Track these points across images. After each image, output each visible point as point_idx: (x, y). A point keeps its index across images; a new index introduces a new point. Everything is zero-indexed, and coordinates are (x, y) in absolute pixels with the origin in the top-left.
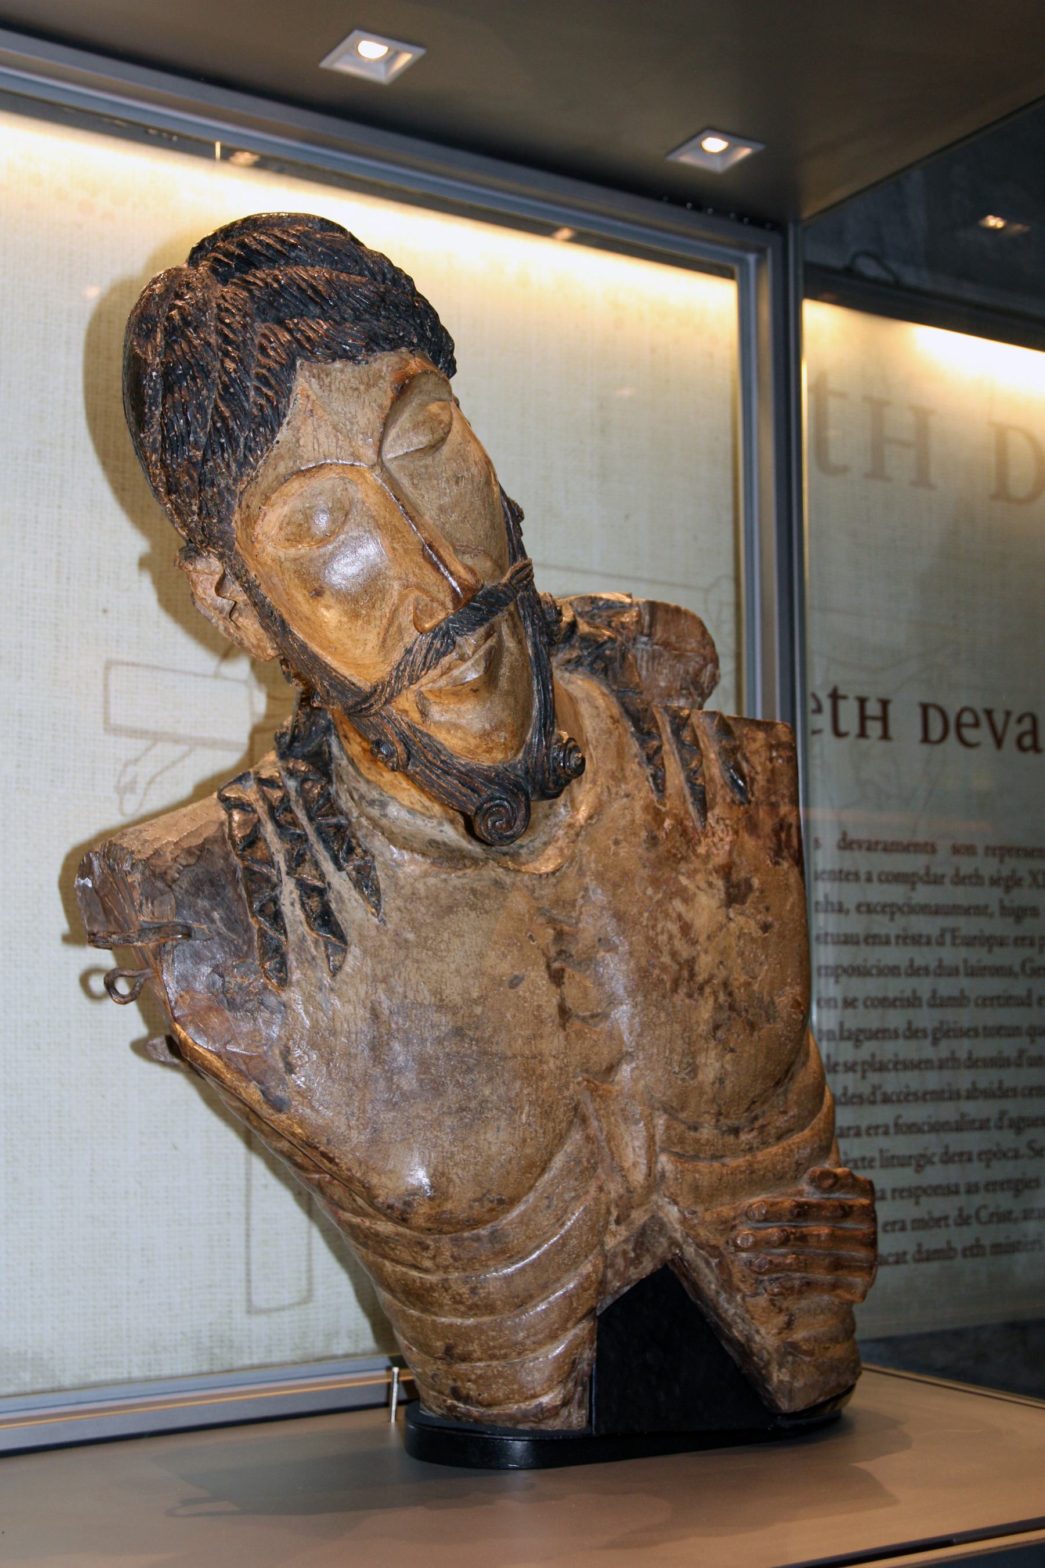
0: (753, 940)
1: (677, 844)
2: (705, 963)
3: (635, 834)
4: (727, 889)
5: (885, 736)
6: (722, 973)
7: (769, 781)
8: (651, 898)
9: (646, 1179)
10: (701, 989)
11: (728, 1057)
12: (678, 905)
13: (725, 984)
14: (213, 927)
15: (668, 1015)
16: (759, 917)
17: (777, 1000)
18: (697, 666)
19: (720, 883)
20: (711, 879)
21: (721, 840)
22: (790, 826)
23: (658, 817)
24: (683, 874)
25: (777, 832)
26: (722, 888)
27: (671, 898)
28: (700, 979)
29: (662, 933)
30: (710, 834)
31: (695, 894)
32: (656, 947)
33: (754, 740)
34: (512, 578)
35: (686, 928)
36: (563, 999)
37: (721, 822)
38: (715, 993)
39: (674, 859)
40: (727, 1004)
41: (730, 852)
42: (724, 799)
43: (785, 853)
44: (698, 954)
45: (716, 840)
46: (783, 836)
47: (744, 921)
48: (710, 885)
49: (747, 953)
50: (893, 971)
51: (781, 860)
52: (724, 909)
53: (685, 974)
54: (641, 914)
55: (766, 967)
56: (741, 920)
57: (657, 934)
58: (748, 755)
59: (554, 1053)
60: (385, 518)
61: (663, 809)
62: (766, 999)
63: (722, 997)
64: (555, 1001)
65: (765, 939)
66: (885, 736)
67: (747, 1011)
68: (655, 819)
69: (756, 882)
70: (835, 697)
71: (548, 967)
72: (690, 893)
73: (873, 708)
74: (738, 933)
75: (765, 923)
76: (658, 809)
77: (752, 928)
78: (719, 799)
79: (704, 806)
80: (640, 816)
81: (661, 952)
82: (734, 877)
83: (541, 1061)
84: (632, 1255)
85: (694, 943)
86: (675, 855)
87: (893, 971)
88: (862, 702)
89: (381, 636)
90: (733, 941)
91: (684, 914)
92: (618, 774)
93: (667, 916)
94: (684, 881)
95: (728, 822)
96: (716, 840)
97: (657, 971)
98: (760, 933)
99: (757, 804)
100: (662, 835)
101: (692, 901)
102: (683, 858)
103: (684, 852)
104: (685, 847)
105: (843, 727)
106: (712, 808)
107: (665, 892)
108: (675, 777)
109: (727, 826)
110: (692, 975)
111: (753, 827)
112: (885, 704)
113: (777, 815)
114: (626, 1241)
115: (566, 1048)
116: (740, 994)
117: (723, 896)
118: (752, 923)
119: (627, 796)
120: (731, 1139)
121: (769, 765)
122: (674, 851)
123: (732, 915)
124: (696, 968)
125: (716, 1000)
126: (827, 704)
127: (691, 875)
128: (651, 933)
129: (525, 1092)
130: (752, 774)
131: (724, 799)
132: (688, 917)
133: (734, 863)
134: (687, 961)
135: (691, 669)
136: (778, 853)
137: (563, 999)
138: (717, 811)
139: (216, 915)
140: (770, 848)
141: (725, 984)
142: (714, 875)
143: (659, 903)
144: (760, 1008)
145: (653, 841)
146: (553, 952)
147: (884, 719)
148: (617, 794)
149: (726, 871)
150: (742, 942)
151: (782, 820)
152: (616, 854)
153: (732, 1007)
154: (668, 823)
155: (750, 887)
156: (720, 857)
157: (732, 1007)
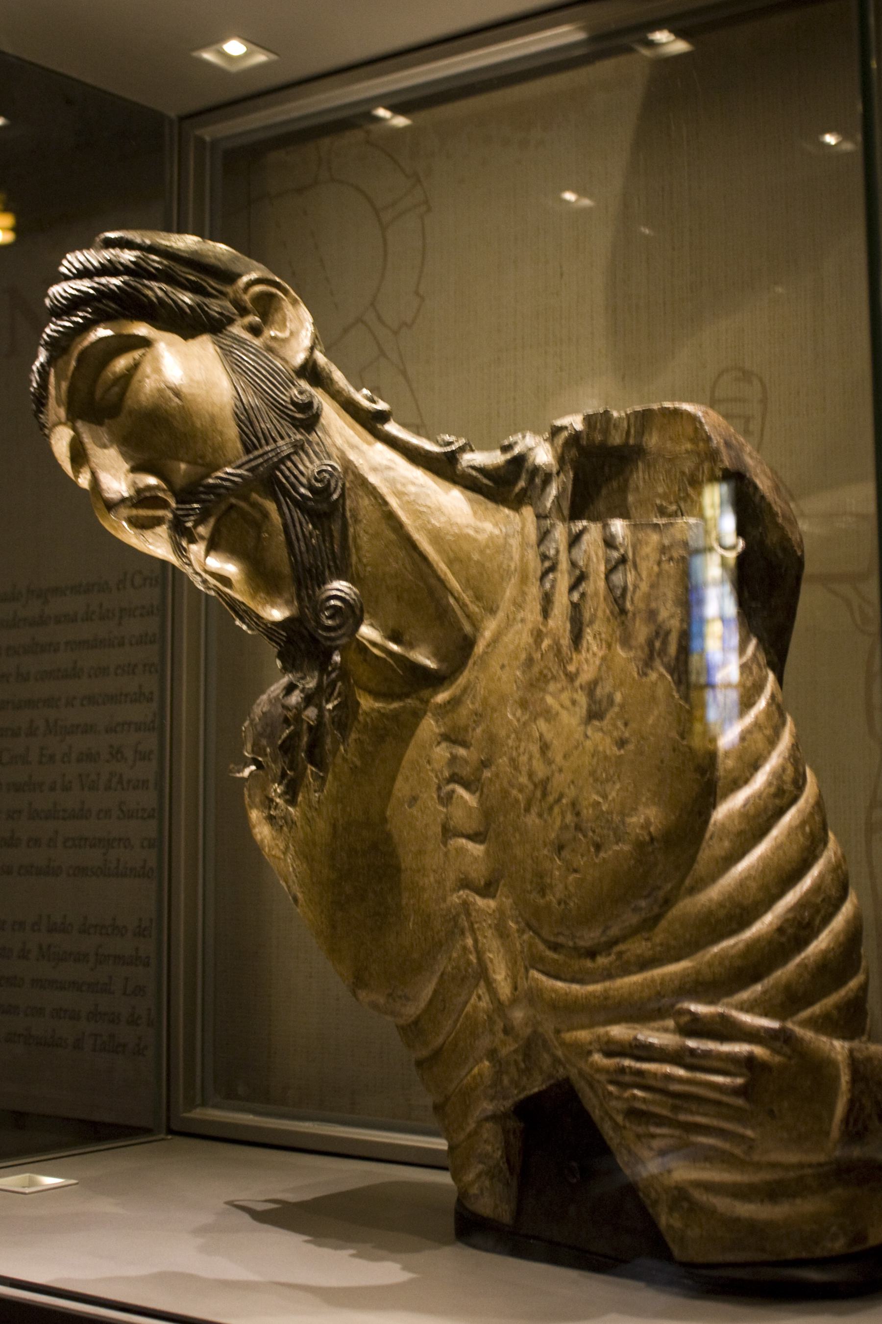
0: (606, 758)
2: (559, 781)
4: (589, 705)
6: (571, 792)
7: (652, 586)
9: (512, 993)
10: (551, 809)
11: (572, 877)
12: (542, 724)
13: (573, 804)
15: (521, 834)
17: (629, 820)
19: (582, 699)
20: (575, 696)
22: (668, 633)
23: (538, 636)
24: (551, 694)
25: (650, 643)
26: (585, 706)
27: (535, 719)
28: (551, 799)
31: (557, 714)
32: (516, 768)
33: (647, 543)
35: (545, 748)
36: (448, 817)
38: (563, 814)
40: (573, 824)
41: (600, 669)
43: (657, 663)
44: (553, 775)
46: (657, 644)
47: (599, 739)
48: (574, 702)
49: (599, 772)
51: (649, 672)
52: (582, 728)
53: (538, 794)
54: (508, 737)
55: (618, 786)
57: (519, 755)
59: (434, 867)
61: (544, 630)
62: (616, 818)
63: (569, 818)
64: (440, 819)
65: (621, 756)
67: (594, 832)
68: (536, 642)
69: (618, 697)
71: (439, 788)
72: (554, 712)
74: (592, 750)
75: (621, 739)
77: (608, 747)
78: (600, 614)
80: (526, 639)
81: (520, 773)
82: (598, 691)
83: (424, 875)
84: (522, 1065)
85: (549, 762)
90: (587, 759)
91: (545, 734)
92: (519, 599)
93: (530, 736)
94: (549, 700)
96: (589, 656)
97: (514, 792)
98: (615, 749)
99: (634, 615)
100: (537, 656)
101: (555, 719)
102: (554, 678)
103: (555, 673)
104: (556, 667)
106: (591, 623)
107: (531, 713)
110: (544, 795)
111: (626, 641)
113: (655, 621)
114: (515, 1051)
115: (445, 863)
116: (587, 813)
117: (584, 711)
118: (608, 740)
119: (523, 621)
120: (589, 964)
121: (656, 568)
122: (545, 671)
123: (589, 733)
124: (549, 787)
125: (562, 821)
127: (553, 695)
128: (514, 754)
129: (412, 902)
132: (548, 736)
133: (601, 678)
135: (687, 471)
136: (648, 663)
137: (448, 817)
138: (596, 627)
144: (609, 829)
145: (530, 661)
146: (446, 774)
149: (591, 689)
150: (595, 760)
151: (660, 627)
152: (499, 679)
153: (578, 828)
154: (546, 643)
155: (611, 701)
157: (578, 828)
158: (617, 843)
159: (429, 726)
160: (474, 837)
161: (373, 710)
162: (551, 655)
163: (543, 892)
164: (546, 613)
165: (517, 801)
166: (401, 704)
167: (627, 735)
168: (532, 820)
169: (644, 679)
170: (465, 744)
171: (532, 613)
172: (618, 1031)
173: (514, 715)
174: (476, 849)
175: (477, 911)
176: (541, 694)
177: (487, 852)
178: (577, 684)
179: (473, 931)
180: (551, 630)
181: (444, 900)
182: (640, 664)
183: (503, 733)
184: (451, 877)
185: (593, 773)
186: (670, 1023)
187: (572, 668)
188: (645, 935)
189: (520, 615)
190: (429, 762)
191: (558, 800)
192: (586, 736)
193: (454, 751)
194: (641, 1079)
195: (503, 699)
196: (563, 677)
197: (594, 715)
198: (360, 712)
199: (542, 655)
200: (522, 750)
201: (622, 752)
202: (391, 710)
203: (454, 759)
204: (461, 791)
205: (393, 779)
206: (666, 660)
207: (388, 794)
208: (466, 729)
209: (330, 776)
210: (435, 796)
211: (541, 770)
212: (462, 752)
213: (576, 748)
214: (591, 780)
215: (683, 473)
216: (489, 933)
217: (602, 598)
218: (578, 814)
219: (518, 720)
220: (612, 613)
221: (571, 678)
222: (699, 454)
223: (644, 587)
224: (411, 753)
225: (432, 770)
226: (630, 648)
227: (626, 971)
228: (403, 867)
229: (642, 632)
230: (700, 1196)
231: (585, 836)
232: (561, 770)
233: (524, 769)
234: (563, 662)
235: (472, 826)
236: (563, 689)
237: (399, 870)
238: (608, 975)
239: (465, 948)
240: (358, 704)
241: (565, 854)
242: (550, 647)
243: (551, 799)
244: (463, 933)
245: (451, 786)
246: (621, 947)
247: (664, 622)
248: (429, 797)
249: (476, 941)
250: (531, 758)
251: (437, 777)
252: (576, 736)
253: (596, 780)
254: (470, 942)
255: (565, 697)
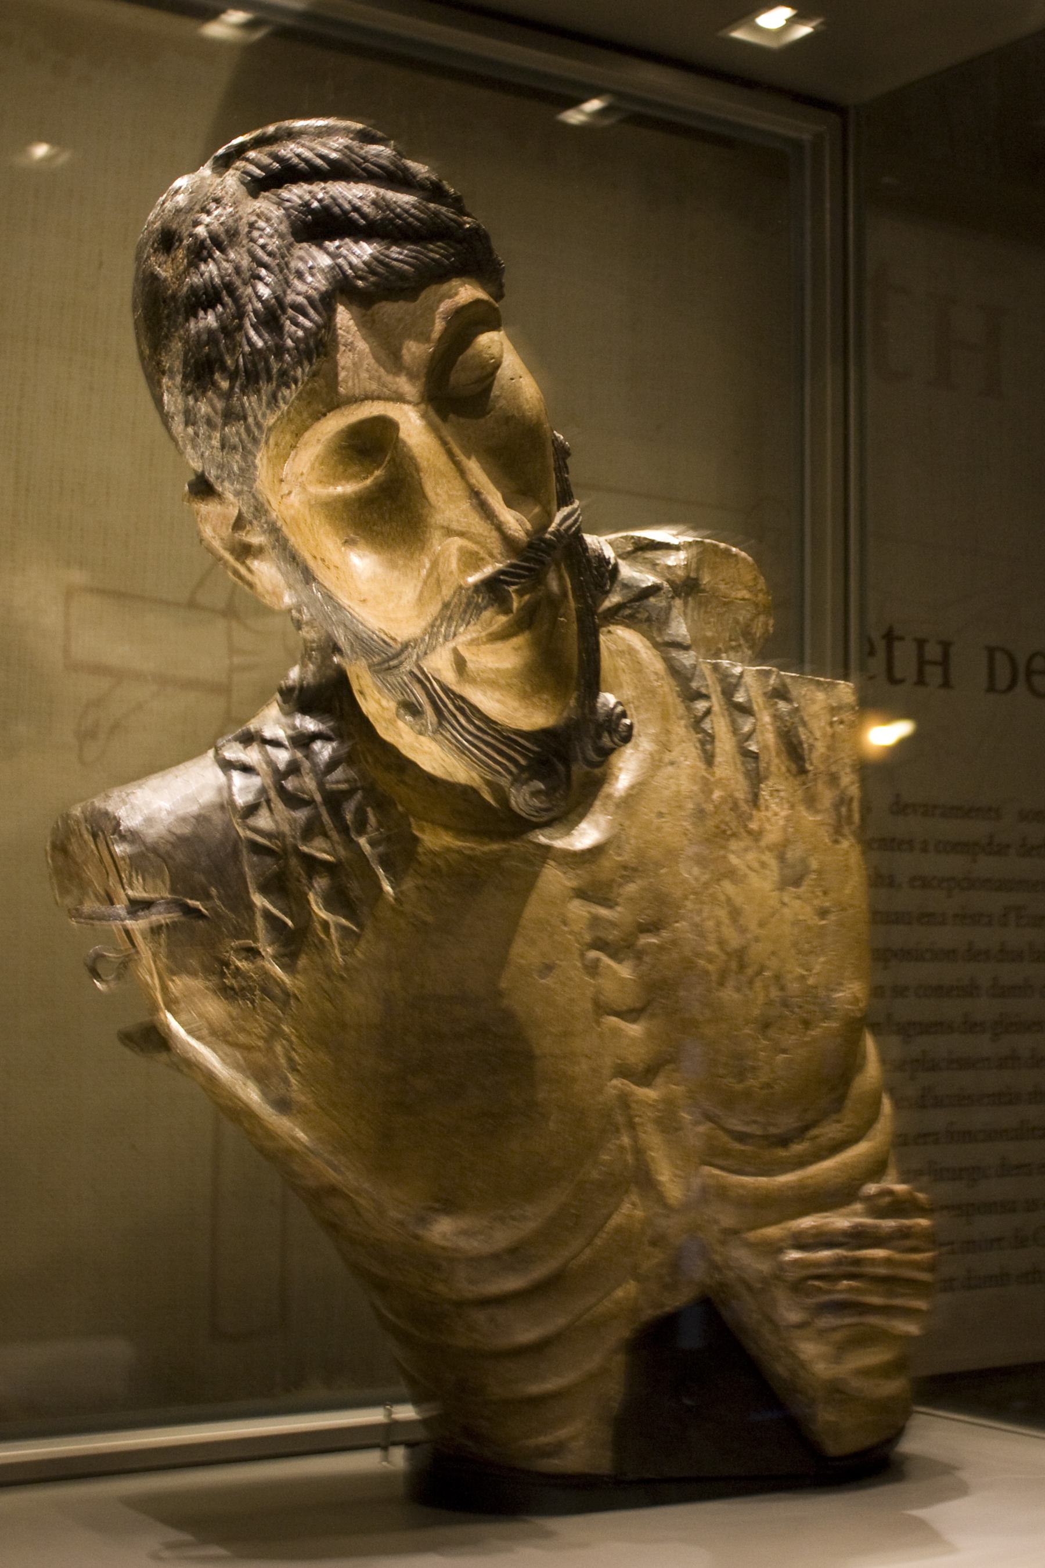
0: (809, 928)
1: (727, 819)
3: (680, 807)
4: (781, 869)
5: (946, 684)
6: (774, 963)
7: (830, 748)
8: (697, 879)
10: (751, 982)
12: (728, 887)
13: (777, 977)
14: (210, 904)
16: (816, 902)
18: (749, 616)
21: (776, 814)
22: (851, 799)
23: (707, 788)
24: (733, 852)
27: (719, 880)
29: (709, 919)
30: (763, 808)
31: (745, 876)
33: (813, 701)
34: (560, 525)
35: (735, 913)
37: (775, 793)
38: (766, 988)
39: (720, 836)
41: (785, 829)
42: (779, 769)
43: (846, 830)
45: (769, 814)
48: (763, 865)
50: (949, 955)
53: (734, 965)
55: (822, 959)
56: (797, 903)
57: (703, 920)
58: (806, 718)
60: (428, 460)
61: (712, 779)
62: (822, 993)
63: (774, 993)
64: (590, 992)
66: (946, 684)
69: (814, 865)
70: (890, 637)
71: (582, 955)
73: (933, 651)
76: (708, 779)
78: (773, 769)
79: (756, 778)
80: (686, 785)
82: (789, 855)
84: (667, 1279)
85: (743, 930)
86: (724, 832)
87: (949, 955)
88: (921, 643)
89: (419, 589)
93: (714, 900)
94: (734, 860)
95: (782, 794)
96: (769, 814)
100: (709, 808)
102: (734, 835)
103: (733, 827)
105: (898, 674)
106: (766, 778)
108: (725, 745)
109: (782, 798)
110: (742, 967)
111: (811, 801)
112: (946, 646)
113: (838, 785)
116: (794, 987)
119: (672, 763)
121: (828, 729)
122: (723, 827)
123: (786, 899)
126: (880, 645)
128: (697, 919)
130: (811, 741)
131: (779, 769)
132: (739, 901)
134: (736, 951)
135: (741, 619)
136: (837, 831)
139: (213, 891)
140: (829, 824)
141: (777, 977)
142: (767, 853)
143: (706, 885)
145: (700, 814)
146: (588, 938)
147: (945, 662)
148: (660, 760)
149: (780, 851)
151: (843, 792)
152: (659, 829)
154: (717, 794)
156: (773, 836)
157: (785, 1004)
158: (823, 1020)
159: (554, 879)
160: (631, 1014)
161: (449, 849)
162: (726, 808)
163: (741, 1075)
164: (709, 759)
165: (707, 973)
166: (504, 846)
167: (827, 904)
168: (728, 994)
169: (838, 846)
170: (607, 902)
171: (687, 754)
172: (807, 1222)
173: (690, 874)
174: (634, 1030)
175: (637, 1102)
176: (722, 853)
177: (650, 1035)
178: (763, 843)
179: (632, 1126)
180: (721, 779)
181: (600, 1090)
182: (831, 831)
183: (678, 893)
184: (608, 1061)
185: (795, 944)
186: (858, 1207)
187: (753, 826)
188: (835, 1117)
189: (667, 757)
190: (565, 924)
191: (759, 973)
192: (784, 904)
193: (593, 910)
194: (854, 1270)
195: (672, 855)
196: (745, 834)
197: (793, 878)
198: (420, 850)
199: (715, 807)
200: (705, 914)
201: (824, 922)
202: (484, 853)
203: (595, 921)
204: (606, 960)
205: (509, 943)
206: (853, 827)
207: (502, 962)
208: (610, 884)
209: (369, 934)
210: (579, 964)
211: (735, 940)
212: (603, 912)
213: (773, 915)
214: (793, 951)
215: (737, 622)
216: (650, 1127)
217: (774, 754)
218: (782, 988)
219: (697, 879)
220: (789, 771)
221: (756, 836)
222: (757, 605)
223: (820, 748)
224: (533, 910)
225: (571, 932)
226: (817, 812)
227: (818, 1156)
228: (538, 1052)
229: (827, 797)
230: (855, 1383)
231: (793, 1012)
232: (757, 939)
233: (712, 937)
234: (744, 819)
235: (628, 1000)
236: (746, 849)
237: (531, 1057)
238: (802, 1162)
239: (622, 1149)
240: (416, 840)
241: (772, 1032)
242: (724, 800)
243: (750, 971)
244: (618, 1130)
245: (593, 954)
246: (815, 1132)
247: (846, 787)
248: (572, 967)
249: (635, 1139)
250: (718, 924)
251: (578, 942)
252: (772, 902)
253: (799, 952)
254: (626, 1140)
255: (751, 856)
